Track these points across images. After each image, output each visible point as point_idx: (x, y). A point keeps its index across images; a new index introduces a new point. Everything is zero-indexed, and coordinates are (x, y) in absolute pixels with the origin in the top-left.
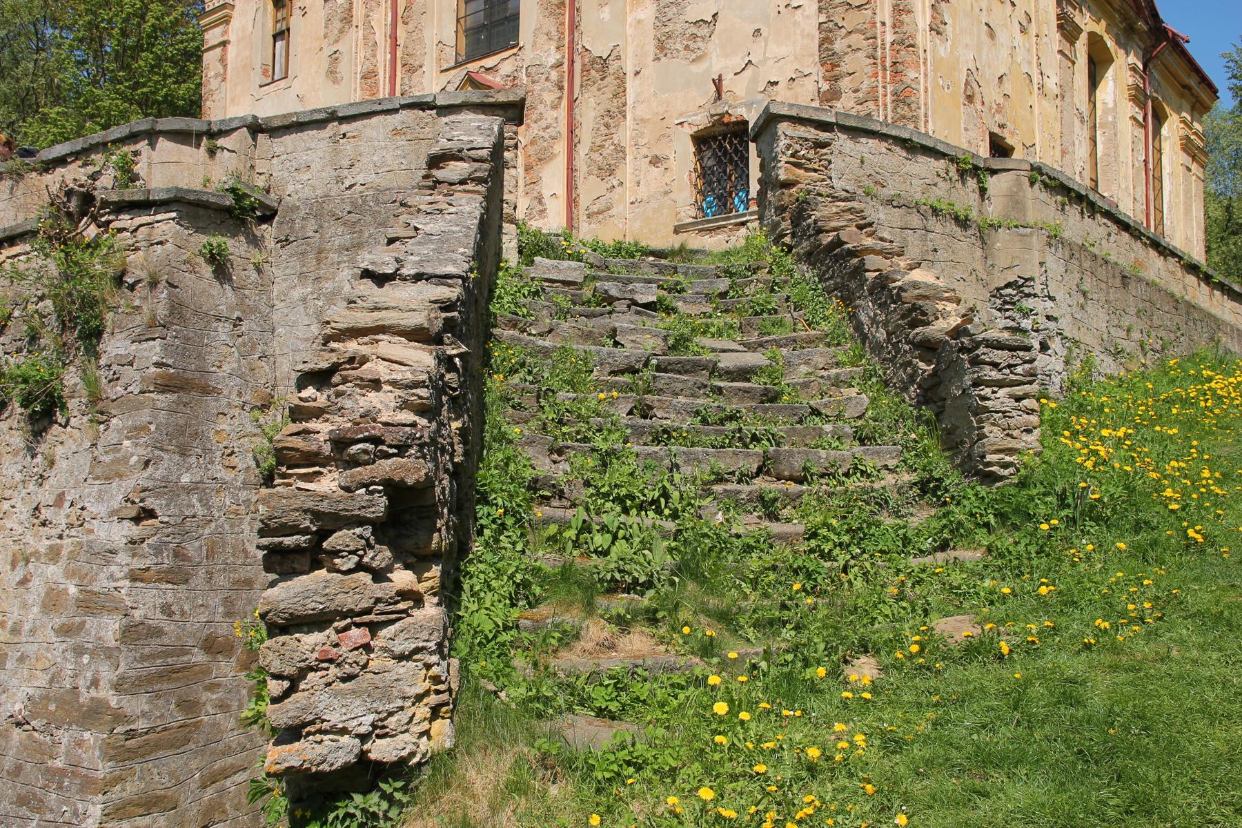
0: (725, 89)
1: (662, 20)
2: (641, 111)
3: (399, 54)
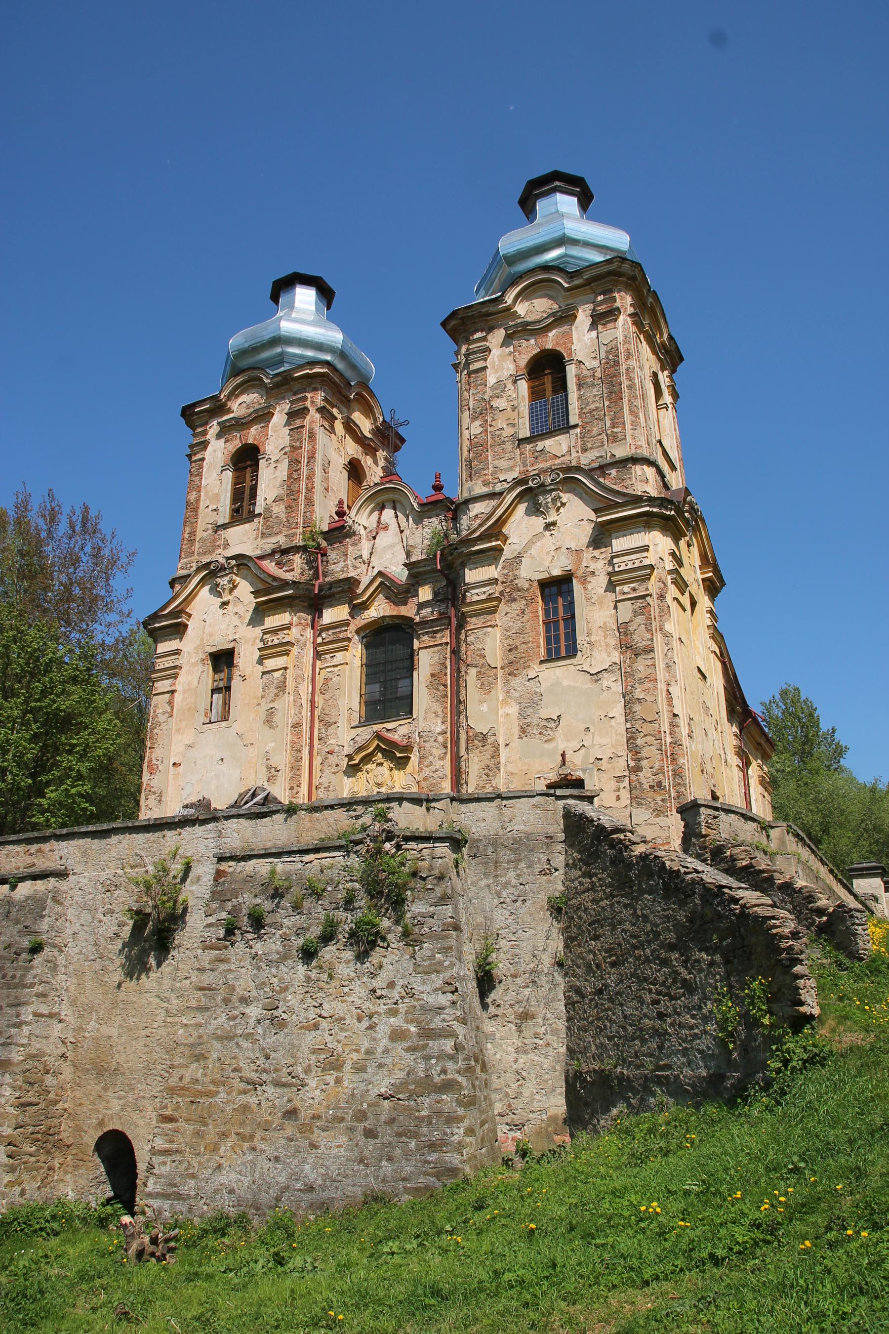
0: (567, 760)
1: (522, 715)
2: (510, 768)
3: (316, 713)
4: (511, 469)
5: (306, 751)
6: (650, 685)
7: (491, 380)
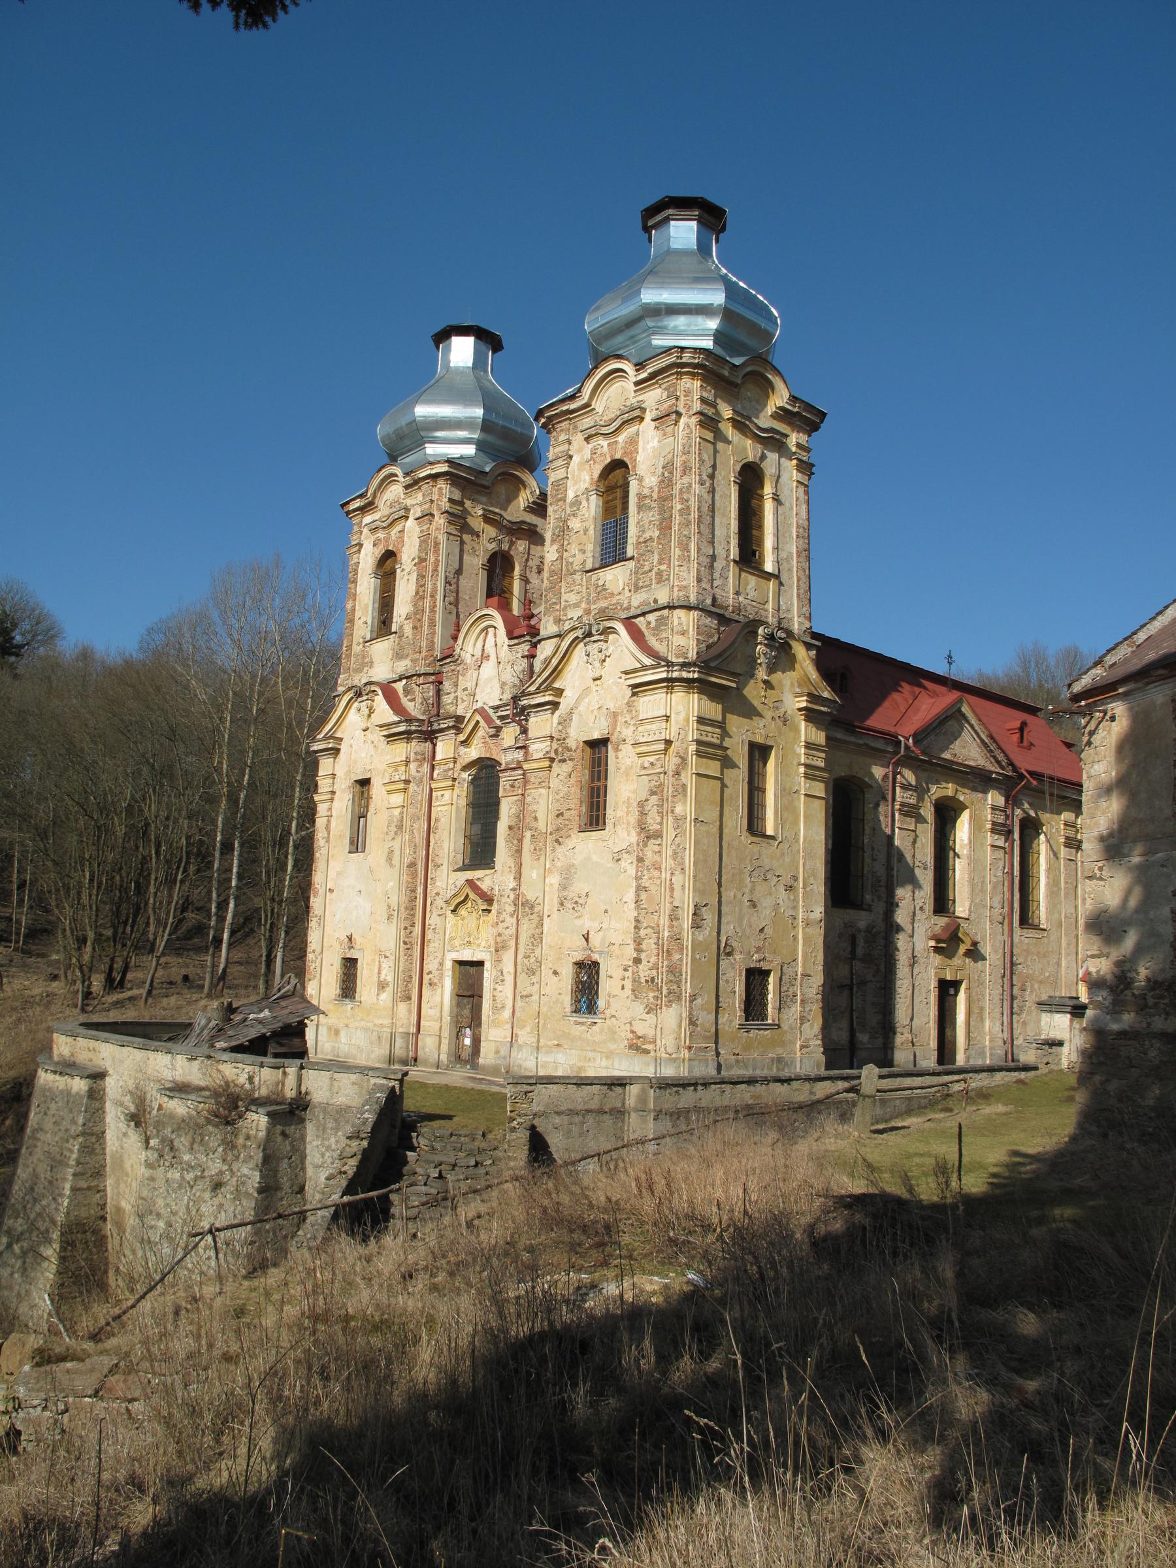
1: (563, 887)
4: (576, 605)
5: (420, 890)
6: (656, 873)
7: (571, 495)
